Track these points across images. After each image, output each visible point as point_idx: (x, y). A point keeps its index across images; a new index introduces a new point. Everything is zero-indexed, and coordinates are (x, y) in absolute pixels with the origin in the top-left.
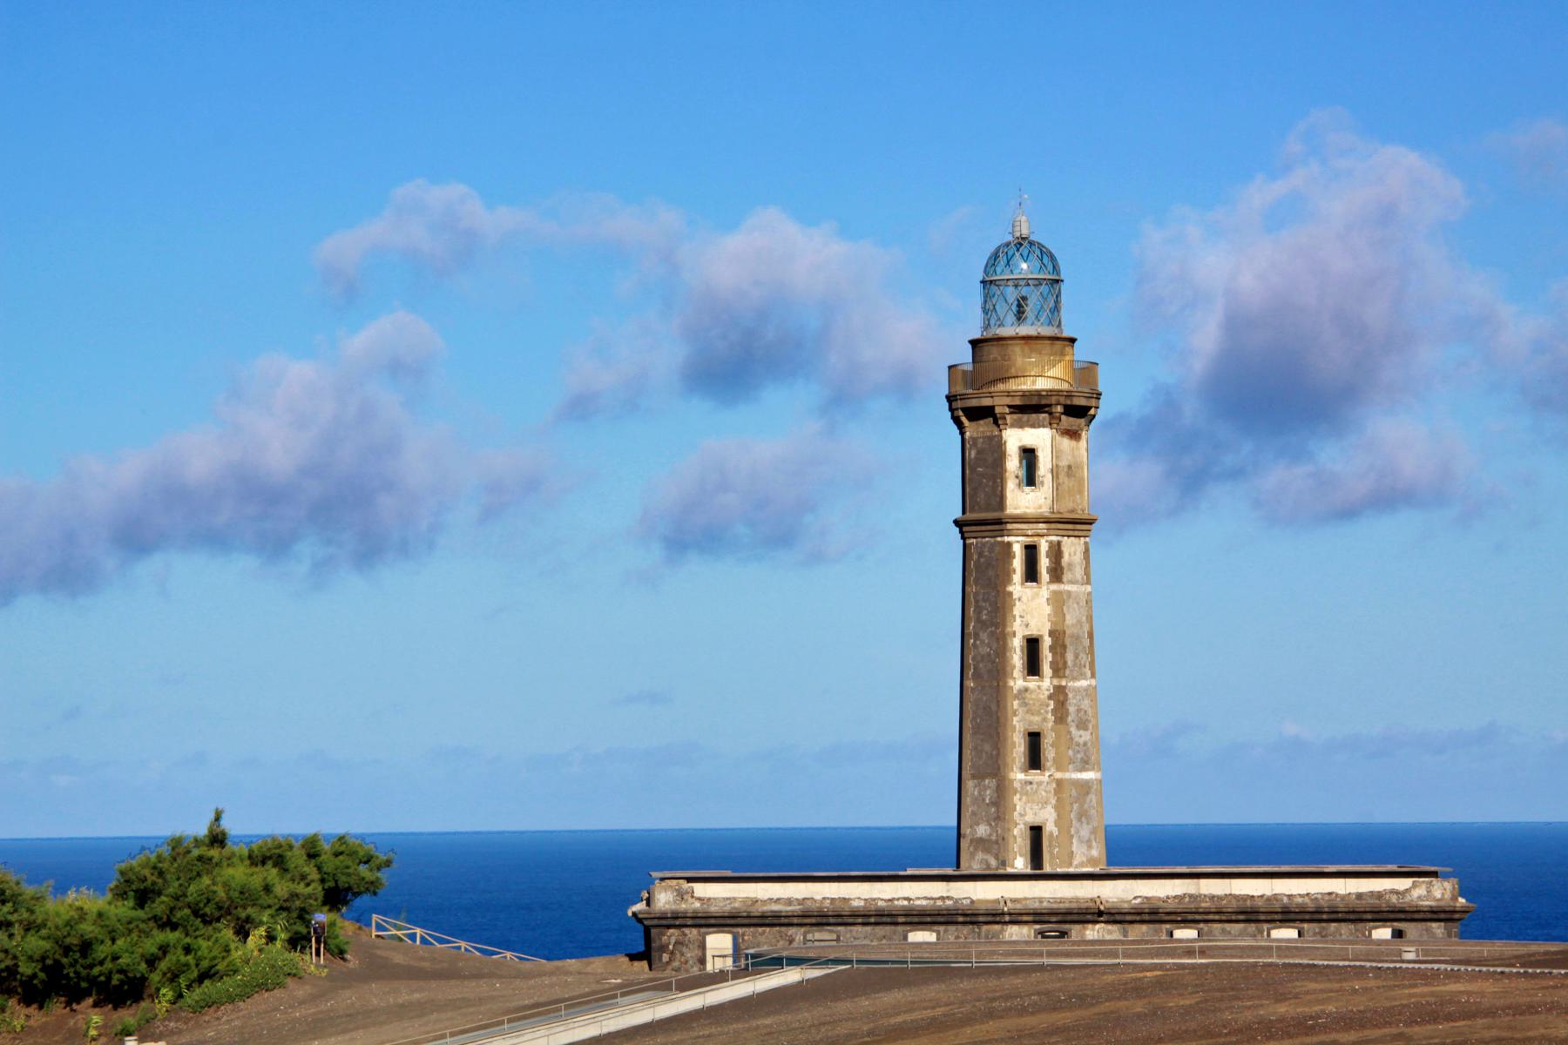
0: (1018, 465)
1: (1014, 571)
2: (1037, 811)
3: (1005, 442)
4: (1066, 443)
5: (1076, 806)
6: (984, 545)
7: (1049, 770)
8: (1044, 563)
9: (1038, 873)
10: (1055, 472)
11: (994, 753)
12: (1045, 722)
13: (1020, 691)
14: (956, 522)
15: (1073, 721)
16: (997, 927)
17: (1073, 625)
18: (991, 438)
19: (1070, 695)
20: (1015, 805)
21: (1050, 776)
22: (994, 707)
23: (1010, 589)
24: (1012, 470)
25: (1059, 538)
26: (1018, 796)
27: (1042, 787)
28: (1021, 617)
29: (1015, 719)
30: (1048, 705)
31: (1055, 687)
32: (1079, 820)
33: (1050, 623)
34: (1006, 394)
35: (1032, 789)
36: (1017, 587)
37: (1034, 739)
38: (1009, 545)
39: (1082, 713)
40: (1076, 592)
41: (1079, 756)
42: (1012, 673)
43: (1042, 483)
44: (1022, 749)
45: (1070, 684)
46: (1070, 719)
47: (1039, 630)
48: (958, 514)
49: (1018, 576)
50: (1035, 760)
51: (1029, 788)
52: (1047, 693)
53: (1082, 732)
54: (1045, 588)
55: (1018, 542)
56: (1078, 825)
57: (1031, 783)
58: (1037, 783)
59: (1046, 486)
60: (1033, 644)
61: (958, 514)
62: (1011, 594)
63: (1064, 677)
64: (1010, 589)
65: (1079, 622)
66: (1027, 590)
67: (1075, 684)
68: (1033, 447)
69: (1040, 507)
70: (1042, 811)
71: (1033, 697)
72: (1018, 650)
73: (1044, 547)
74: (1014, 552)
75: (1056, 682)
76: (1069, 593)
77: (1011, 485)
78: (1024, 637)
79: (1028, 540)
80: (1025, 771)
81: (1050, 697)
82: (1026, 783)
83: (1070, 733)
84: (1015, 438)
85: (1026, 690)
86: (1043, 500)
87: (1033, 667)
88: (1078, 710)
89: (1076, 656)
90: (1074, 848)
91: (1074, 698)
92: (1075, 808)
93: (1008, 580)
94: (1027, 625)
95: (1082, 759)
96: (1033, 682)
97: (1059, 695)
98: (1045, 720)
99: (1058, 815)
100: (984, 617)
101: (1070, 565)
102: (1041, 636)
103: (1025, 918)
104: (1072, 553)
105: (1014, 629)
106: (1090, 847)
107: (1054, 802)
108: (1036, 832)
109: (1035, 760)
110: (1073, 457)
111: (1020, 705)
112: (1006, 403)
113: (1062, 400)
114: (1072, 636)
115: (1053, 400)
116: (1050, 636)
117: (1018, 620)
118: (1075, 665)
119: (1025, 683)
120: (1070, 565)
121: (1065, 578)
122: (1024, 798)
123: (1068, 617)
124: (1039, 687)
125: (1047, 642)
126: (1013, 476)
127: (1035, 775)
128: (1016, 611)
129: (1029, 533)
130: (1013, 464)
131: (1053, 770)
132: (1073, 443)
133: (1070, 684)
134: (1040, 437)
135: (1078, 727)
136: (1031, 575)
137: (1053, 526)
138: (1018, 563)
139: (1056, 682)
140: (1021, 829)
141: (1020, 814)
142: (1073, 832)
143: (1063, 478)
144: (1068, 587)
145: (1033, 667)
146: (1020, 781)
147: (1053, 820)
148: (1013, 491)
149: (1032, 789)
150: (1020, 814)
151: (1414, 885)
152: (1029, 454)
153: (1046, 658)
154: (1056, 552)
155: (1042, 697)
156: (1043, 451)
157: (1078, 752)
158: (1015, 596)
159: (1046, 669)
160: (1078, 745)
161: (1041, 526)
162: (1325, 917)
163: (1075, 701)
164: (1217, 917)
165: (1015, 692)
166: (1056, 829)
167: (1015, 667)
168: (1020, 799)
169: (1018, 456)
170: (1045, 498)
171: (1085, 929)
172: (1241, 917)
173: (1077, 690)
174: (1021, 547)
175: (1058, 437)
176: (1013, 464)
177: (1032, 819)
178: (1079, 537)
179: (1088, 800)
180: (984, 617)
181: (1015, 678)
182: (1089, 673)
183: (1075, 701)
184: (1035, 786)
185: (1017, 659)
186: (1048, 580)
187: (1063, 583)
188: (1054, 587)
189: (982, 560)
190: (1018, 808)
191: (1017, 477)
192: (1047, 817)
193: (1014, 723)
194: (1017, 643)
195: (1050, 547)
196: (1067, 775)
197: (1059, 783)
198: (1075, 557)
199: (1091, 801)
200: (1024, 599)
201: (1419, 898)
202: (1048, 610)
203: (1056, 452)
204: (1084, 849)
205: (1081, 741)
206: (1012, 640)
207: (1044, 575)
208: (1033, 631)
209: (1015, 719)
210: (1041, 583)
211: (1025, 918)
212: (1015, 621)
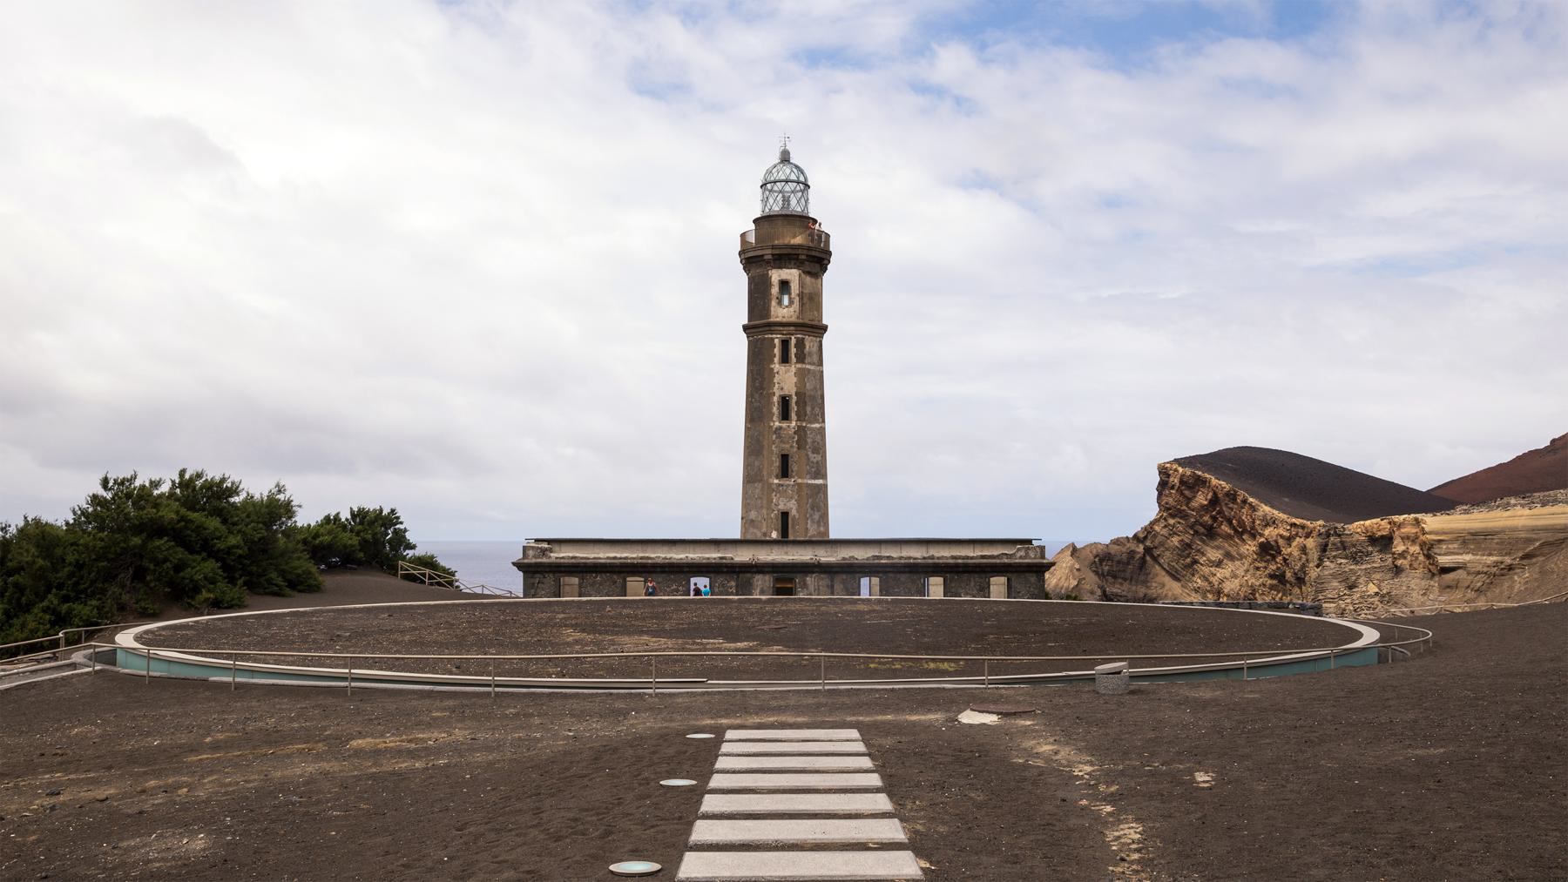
4: (808, 279)
5: (810, 501)
6: (757, 340)
7: (793, 477)
8: (793, 350)
9: (784, 540)
10: (801, 295)
12: (791, 447)
13: (776, 429)
14: (746, 328)
16: (749, 575)
17: (811, 390)
18: (763, 275)
22: (761, 438)
23: (773, 366)
26: (774, 493)
30: (794, 438)
32: (812, 509)
36: (776, 366)
37: (785, 459)
38: (773, 339)
44: (777, 464)
46: (808, 447)
48: (746, 322)
49: (776, 360)
50: (785, 472)
52: (793, 430)
53: (815, 455)
54: (793, 366)
56: (812, 512)
57: (782, 485)
60: (785, 401)
61: (746, 322)
62: (773, 369)
63: (805, 420)
64: (773, 366)
65: (815, 388)
69: (791, 317)
72: (776, 404)
73: (793, 341)
76: (809, 370)
77: (774, 303)
80: (777, 477)
81: (795, 433)
82: (779, 484)
83: (807, 455)
84: (776, 275)
85: (781, 428)
87: (785, 416)
89: (813, 409)
90: (809, 526)
93: (772, 362)
94: (782, 389)
96: (784, 425)
97: (801, 431)
98: (792, 447)
101: (809, 353)
102: (791, 395)
103: (767, 570)
106: (819, 526)
108: (785, 515)
109: (785, 472)
110: (813, 287)
111: (777, 438)
113: (805, 252)
114: (810, 396)
115: (800, 251)
116: (796, 395)
117: (777, 385)
118: (812, 414)
120: (809, 353)
122: (778, 495)
123: (808, 384)
125: (795, 398)
127: (785, 482)
128: (775, 381)
129: (785, 332)
130: (775, 290)
132: (813, 280)
134: (792, 274)
135: (813, 453)
136: (785, 359)
137: (799, 329)
138: (777, 351)
143: (805, 300)
144: (807, 366)
145: (785, 416)
151: (1019, 550)
152: (785, 285)
154: (800, 344)
157: (813, 467)
158: (775, 371)
159: (793, 416)
160: (812, 462)
161: (792, 328)
162: (961, 569)
164: (891, 570)
171: (807, 576)
172: (907, 569)
173: (813, 429)
175: (803, 275)
176: (775, 290)
177: (782, 507)
182: (821, 420)
184: (785, 488)
185: (776, 410)
188: (799, 366)
192: (792, 506)
194: (775, 399)
196: (805, 481)
197: (799, 485)
201: (1021, 557)
202: (795, 380)
203: (802, 284)
204: (815, 526)
205: (815, 460)
208: (786, 392)
211: (767, 570)
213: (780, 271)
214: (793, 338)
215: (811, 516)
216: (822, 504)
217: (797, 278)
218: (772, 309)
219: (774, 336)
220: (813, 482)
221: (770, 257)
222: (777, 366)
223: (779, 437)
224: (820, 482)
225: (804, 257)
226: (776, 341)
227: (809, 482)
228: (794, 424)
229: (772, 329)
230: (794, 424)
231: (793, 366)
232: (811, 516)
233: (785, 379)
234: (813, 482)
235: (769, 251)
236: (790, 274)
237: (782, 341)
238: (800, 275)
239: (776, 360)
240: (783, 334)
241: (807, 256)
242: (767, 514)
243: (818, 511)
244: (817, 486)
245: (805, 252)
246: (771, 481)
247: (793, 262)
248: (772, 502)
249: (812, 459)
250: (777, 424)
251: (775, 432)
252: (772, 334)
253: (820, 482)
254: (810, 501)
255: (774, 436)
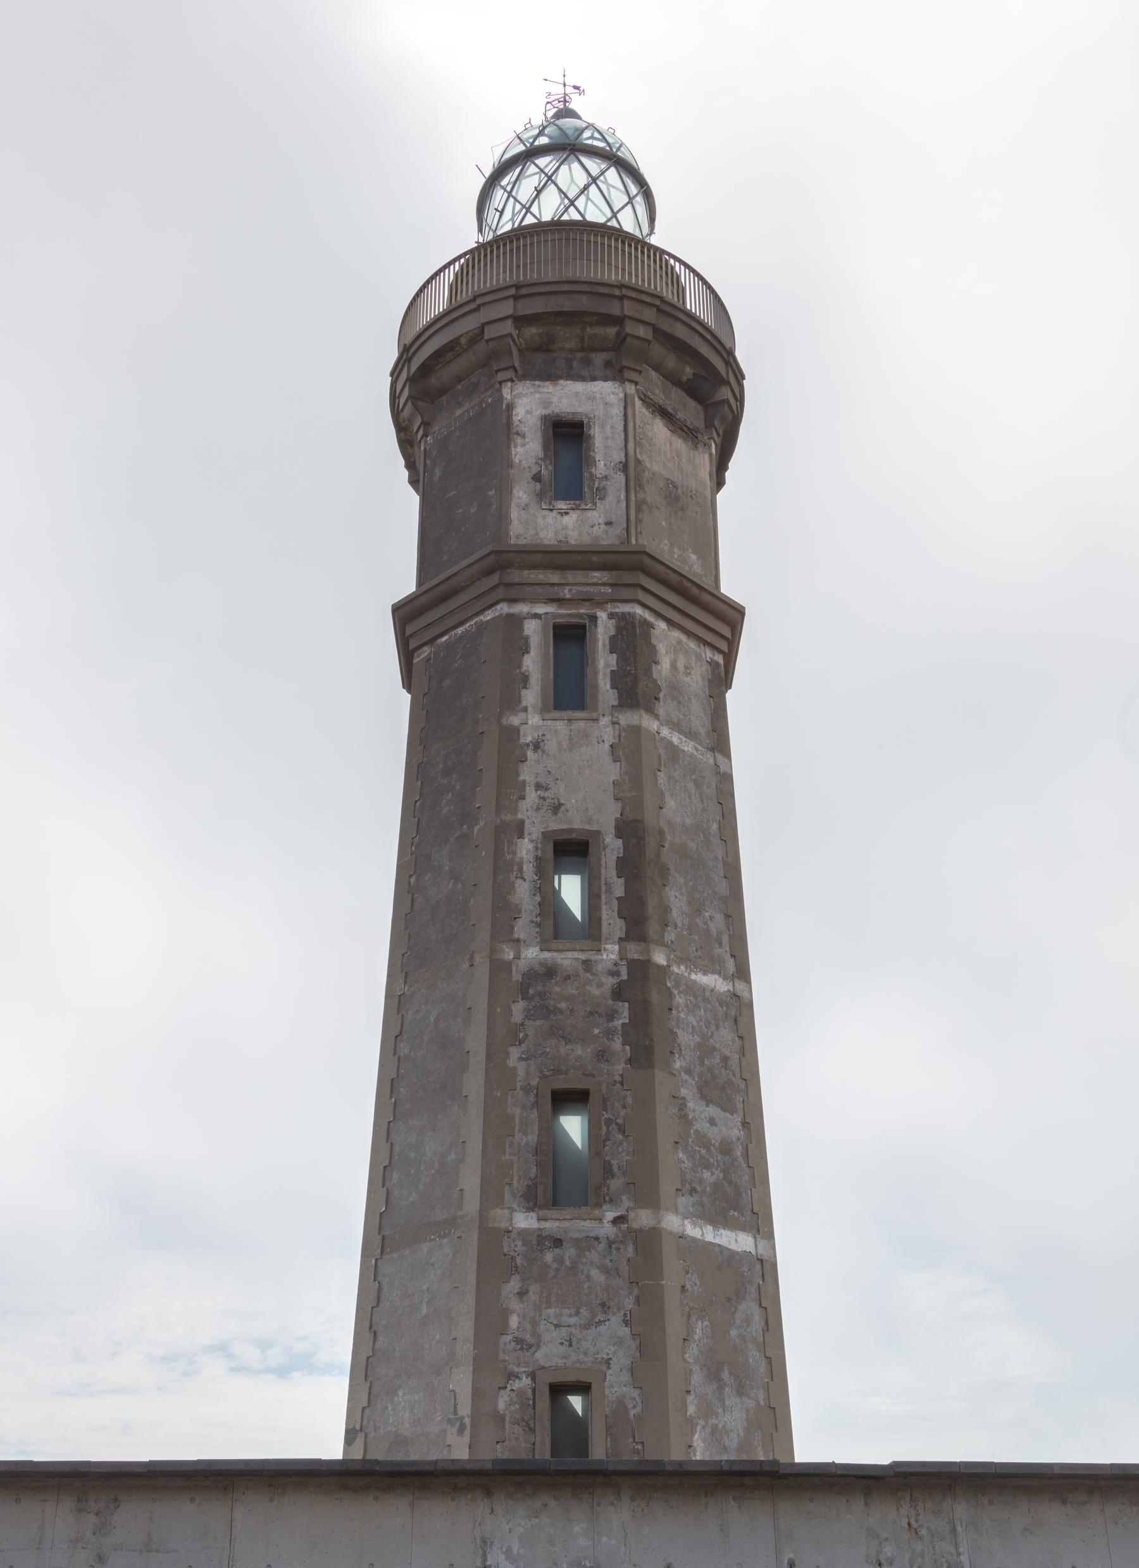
0: (541, 454)
1: (525, 680)
2: (577, 1332)
3: (510, 407)
7: (613, 1201)
8: (604, 661)
11: (452, 1156)
15: (689, 1072)
19: (679, 1000)
20: (506, 1313)
21: (617, 1221)
23: (515, 720)
24: (525, 464)
25: (648, 616)
26: (514, 1284)
27: (593, 1256)
28: (538, 787)
29: (515, 1052)
30: (612, 1015)
31: (632, 965)
32: (714, 1375)
33: (619, 805)
34: (513, 291)
35: (560, 1261)
38: (514, 623)
39: (717, 1060)
40: (691, 755)
41: (706, 1175)
42: (513, 927)
43: (601, 493)
45: (678, 969)
46: (678, 1064)
47: (589, 822)
49: (531, 696)
51: (549, 1257)
52: (610, 981)
53: (713, 1111)
54: (605, 721)
55: (536, 616)
57: (558, 1242)
58: (577, 1242)
59: (611, 499)
62: (513, 732)
64: (515, 720)
66: (560, 726)
67: (693, 977)
68: (578, 418)
70: (592, 1331)
71: (571, 990)
73: (604, 629)
74: (527, 639)
75: (634, 951)
77: (522, 494)
78: (546, 835)
79: (564, 613)
80: (531, 1201)
81: (618, 993)
85: (550, 972)
86: (603, 527)
88: (700, 1046)
89: (697, 910)
91: (692, 1009)
92: (698, 1333)
94: (556, 808)
95: (716, 1186)
98: (603, 1055)
99: (640, 1348)
100: (445, 811)
101: (676, 690)
104: (680, 665)
105: (520, 816)
107: (629, 1303)
111: (529, 1015)
112: (510, 312)
113: (649, 315)
115: (629, 308)
116: (619, 834)
117: (532, 796)
118: (692, 928)
119: (546, 955)
121: (662, 709)
122: (534, 1290)
124: (587, 965)
126: (528, 476)
128: (527, 774)
129: (566, 593)
131: (626, 1202)
132: (679, 444)
133: (678, 969)
138: (533, 663)
139: (634, 951)
140: (521, 1393)
141: (518, 1341)
142: (691, 1410)
146: (524, 1233)
147: (626, 1362)
148: (525, 508)
149: (560, 1261)
150: (518, 1341)
153: (609, 890)
155: (596, 992)
156: (602, 427)
157: (707, 1166)
161: (597, 575)
163: (693, 1020)
165: (517, 977)
166: (635, 1393)
167: (520, 911)
168: (522, 1294)
169: (539, 435)
170: (609, 524)
173: (692, 989)
174: (544, 627)
178: (706, 643)
179: (739, 1317)
180: (445, 811)
181: (518, 941)
182: (731, 966)
183: (693, 1020)
184: (569, 1253)
186: (616, 703)
187: (657, 717)
189: (447, 683)
190: (514, 1321)
191: (537, 478)
193: (512, 1062)
195: (619, 629)
198: (687, 679)
199: (748, 1321)
200: (551, 745)
202: (613, 771)
205: (715, 1134)
206: (510, 843)
207: (606, 691)
208: (574, 821)
209: (515, 1052)
210: (596, 709)
212: (523, 798)
213: (548, 387)
214: (602, 615)
215: (707, 1411)
216: (754, 1356)
217: (617, 411)
218: (514, 514)
219: (522, 608)
220: (710, 1234)
221: (508, 327)
222: (534, 720)
223: (543, 1010)
224: (742, 1242)
225: (642, 331)
226: (531, 628)
227: (692, 1231)
228: (610, 953)
229: (515, 576)
230: (610, 953)
231: (605, 721)
232: (707, 1411)
233: (568, 337)
234: (710, 1234)
235: (507, 308)
236: (591, 398)
237: (556, 627)
238: (627, 401)
239: (531, 696)
240: (558, 601)
241: (656, 330)
242: (477, 1394)
243: (740, 1392)
244: (731, 1259)
245: (649, 315)
246: (499, 1217)
247: (599, 358)
248: (504, 1329)
249: (701, 1126)
250: (532, 953)
251: (523, 991)
252: (513, 601)
253: (742, 1242)
254: (700, 1329)
255: (518, 1009)
